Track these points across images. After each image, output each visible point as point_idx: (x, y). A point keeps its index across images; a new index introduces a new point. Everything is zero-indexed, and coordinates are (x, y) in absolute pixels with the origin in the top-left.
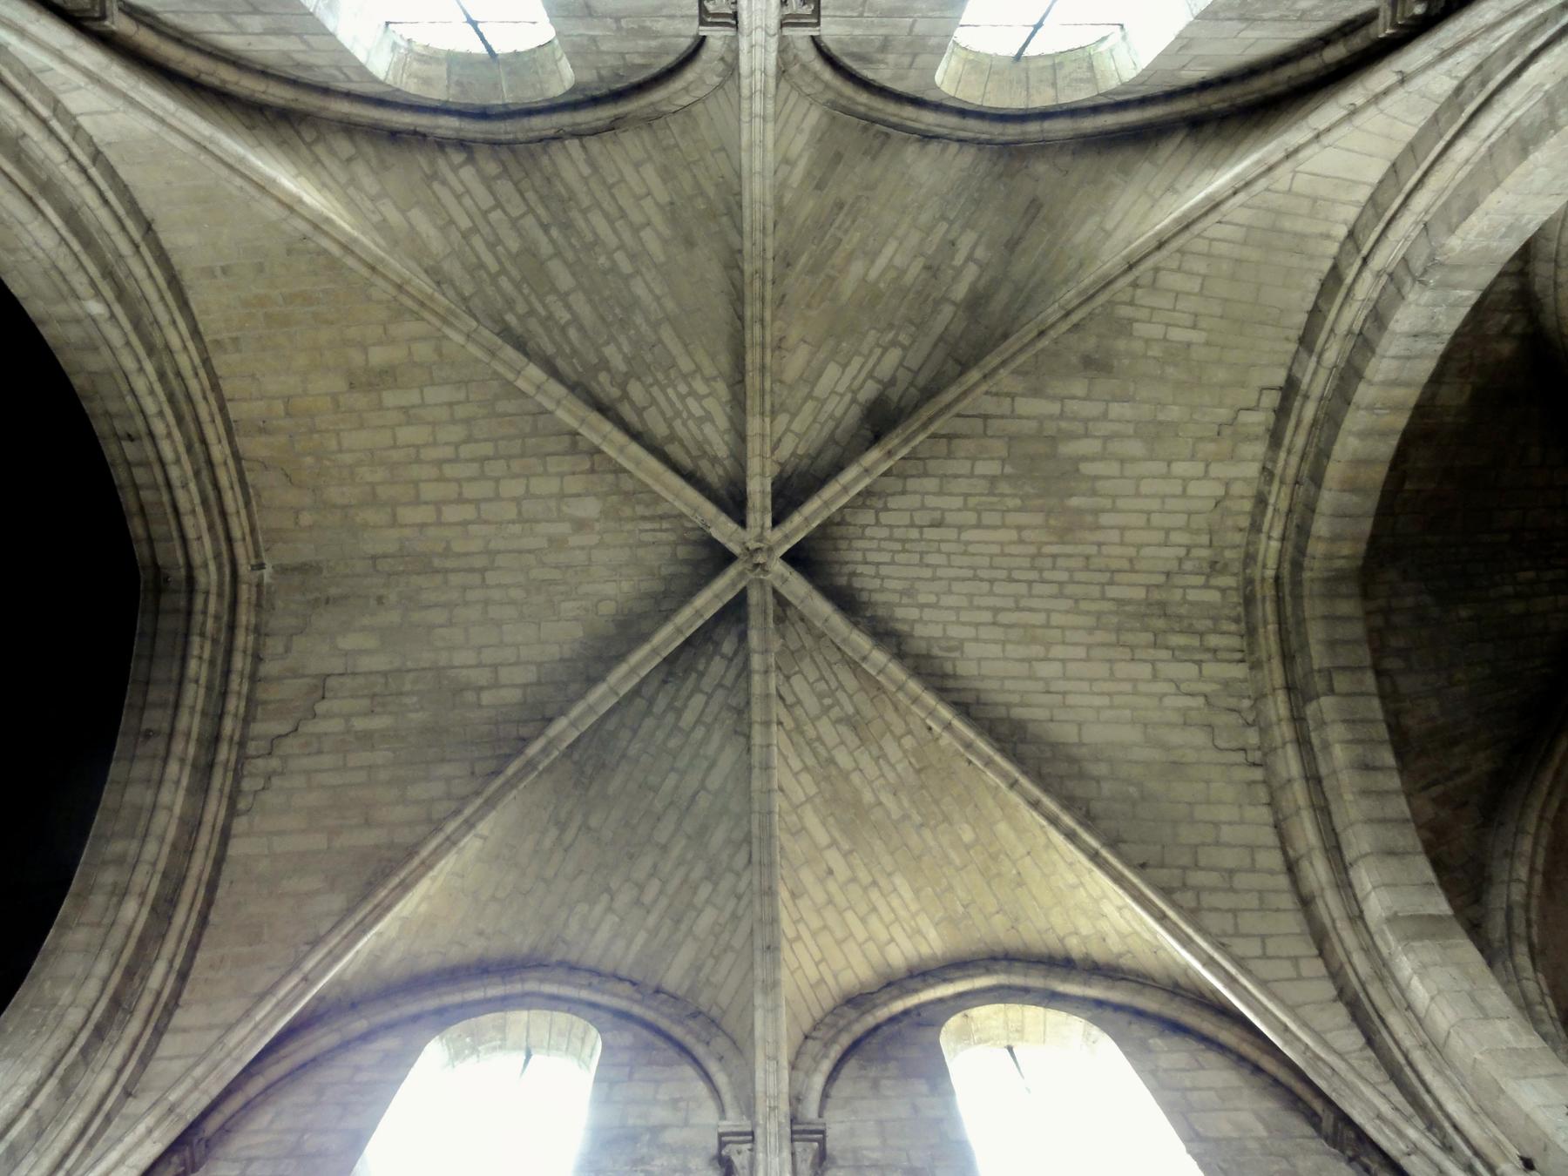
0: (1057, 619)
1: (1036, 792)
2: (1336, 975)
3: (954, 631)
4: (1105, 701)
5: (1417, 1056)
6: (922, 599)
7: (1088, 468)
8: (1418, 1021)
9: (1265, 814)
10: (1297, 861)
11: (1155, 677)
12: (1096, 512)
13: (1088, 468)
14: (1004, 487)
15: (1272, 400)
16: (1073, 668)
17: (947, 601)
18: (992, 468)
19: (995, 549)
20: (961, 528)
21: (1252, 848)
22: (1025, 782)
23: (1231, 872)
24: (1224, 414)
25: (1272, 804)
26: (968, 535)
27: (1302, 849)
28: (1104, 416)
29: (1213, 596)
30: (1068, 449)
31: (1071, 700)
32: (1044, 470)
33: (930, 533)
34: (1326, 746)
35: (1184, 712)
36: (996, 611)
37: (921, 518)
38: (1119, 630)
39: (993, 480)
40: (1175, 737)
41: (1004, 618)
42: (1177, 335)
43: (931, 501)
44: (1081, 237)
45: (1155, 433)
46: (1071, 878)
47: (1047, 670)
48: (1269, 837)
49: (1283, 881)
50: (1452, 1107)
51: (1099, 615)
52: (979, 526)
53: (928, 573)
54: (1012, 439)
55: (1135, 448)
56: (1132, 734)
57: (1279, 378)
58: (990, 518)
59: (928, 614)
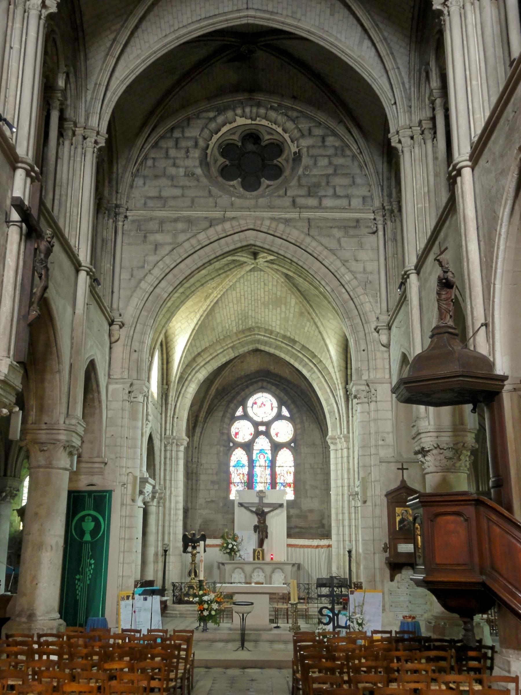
0: (243, 305)
1: (204, 315)
2: (184, 370)
3: (238, 290)
4: (225, 314)
5: (181, 395)
6: (246, 283)
7: (279, 309)
8: (185, 390)
9: (208, 345)
10: (201, 356)
11: (232, 321)
12: (268, 308)
13: (279, 309)
14: (274, 296)
15: (292, 337)
16: (232, 309)
17: (246, 288)
18: (279, 293)
19: (259, 293)
20: (264, 289)
21: (201, 346)
22: (206, 313)
23: (196, 346)
24: (290, 330)
25: (210, 346)
26: (262, 290)
27: (205, 357)
28: (290, 312)
29: (250, 323)
30: (283, 307)
31: (225, 310)
32: (277, 302)
33: (262, 284)
34: (224, 356)
35: (225, 326)
36: (244, 295)
37: (266, 282)
38: (241, 314)
39: (276, 294)
40: (220, 327)
41: (243, 297)
42: (306, 329)
43: (270, 284)
44: (329, 315)
45: (287, 320)
46: (184, 316)
47: (231, 305)
48: (203, 348)
49: (196, 353)
50: (178, 404)
51: (245, 310)
52: (264, 291)
53: (252, 283)
54: (286, 298)
55: (283, 315)
56: (219, 320)
57: (297, 339)
58: (266, 293)
59: (242, 285)
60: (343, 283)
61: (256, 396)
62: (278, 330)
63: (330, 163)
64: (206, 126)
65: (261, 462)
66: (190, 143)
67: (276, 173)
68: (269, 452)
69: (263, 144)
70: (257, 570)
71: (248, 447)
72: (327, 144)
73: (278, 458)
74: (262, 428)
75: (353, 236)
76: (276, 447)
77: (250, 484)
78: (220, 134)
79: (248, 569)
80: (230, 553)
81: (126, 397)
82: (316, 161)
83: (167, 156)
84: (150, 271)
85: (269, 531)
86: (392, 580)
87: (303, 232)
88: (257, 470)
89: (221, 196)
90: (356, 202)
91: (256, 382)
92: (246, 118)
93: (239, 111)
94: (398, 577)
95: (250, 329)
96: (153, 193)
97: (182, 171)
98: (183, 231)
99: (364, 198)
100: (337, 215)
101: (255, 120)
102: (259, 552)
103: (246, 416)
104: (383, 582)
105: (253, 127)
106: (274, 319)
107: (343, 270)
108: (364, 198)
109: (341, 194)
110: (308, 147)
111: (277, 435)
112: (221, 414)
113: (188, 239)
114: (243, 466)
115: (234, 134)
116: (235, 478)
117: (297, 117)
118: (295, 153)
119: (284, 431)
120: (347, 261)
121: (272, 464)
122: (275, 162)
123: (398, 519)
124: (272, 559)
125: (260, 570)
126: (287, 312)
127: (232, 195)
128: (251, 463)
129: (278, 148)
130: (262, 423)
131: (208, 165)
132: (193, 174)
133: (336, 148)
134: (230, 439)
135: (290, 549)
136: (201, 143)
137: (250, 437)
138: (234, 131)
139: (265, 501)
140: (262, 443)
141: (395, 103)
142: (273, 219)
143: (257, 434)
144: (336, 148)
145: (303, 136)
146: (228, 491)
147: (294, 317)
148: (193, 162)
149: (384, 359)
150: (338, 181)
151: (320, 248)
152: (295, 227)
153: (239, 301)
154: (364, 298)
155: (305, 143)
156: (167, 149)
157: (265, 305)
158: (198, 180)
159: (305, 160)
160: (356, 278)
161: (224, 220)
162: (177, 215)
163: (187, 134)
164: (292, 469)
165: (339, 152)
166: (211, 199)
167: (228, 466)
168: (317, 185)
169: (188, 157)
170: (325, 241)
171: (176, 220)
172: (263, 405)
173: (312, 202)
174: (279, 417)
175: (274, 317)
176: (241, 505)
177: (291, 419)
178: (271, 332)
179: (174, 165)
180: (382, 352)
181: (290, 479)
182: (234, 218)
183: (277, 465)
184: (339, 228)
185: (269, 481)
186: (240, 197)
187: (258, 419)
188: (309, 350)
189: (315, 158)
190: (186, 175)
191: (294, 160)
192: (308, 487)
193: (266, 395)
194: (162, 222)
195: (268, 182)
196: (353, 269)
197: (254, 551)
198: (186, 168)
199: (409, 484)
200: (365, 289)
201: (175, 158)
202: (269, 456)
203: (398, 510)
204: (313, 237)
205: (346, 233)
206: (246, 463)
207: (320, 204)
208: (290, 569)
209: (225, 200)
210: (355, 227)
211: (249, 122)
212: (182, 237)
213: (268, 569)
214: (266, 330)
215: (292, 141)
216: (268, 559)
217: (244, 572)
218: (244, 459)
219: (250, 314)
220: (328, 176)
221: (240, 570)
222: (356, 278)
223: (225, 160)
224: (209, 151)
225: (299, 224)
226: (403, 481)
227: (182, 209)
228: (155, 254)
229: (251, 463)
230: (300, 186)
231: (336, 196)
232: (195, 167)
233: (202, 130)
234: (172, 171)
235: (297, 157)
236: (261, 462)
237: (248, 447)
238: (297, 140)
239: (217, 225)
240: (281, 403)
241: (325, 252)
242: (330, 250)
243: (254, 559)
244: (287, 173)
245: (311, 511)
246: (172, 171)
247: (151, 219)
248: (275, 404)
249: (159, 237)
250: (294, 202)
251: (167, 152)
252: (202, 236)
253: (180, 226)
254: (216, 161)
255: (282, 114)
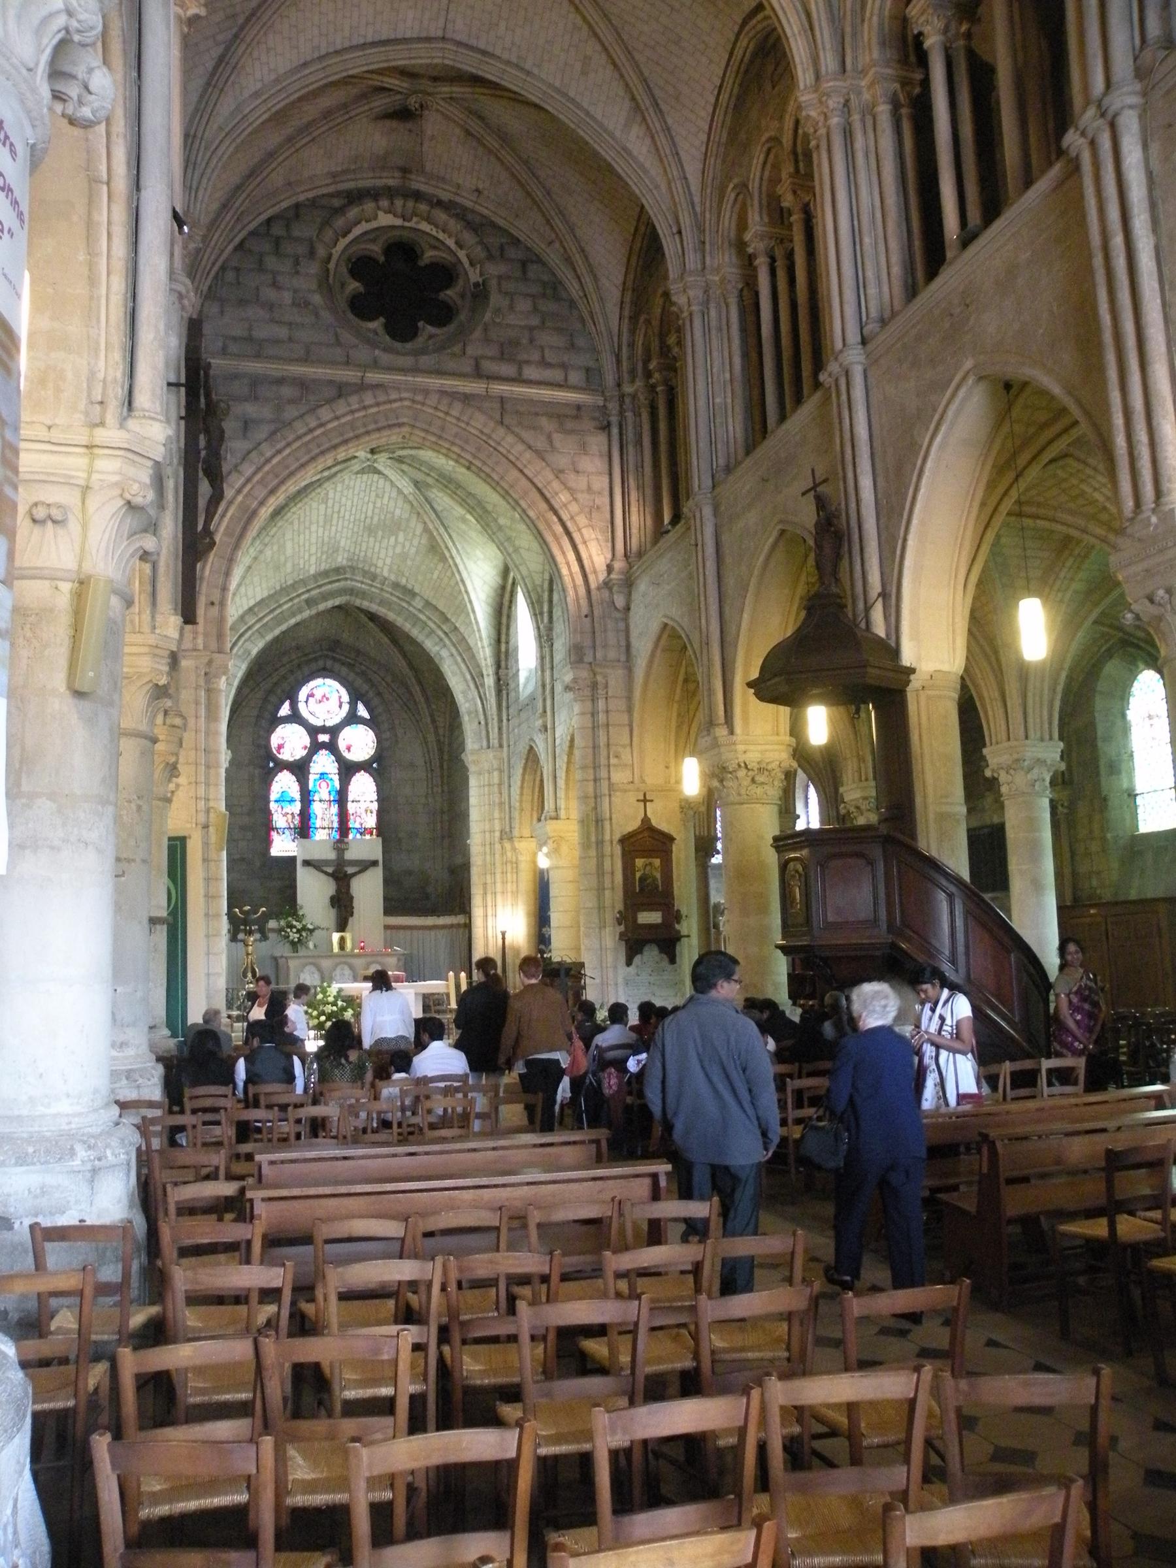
9: (265, 594)
13: (393, 539)
15: (409, 586)
18: (398, 512)
32: (394, 527)
37: (380, 492)
40: (289, 565)
42: (436, 574)
44: (478, 552)
47: (314, 528)
54: (408, 520)
55: (398, 550)
57: (417, 590)
60: (556, 506)
61: (312, 684)
62: (386, 574)
63: (535, 309)
64: (326, 223)
65: (323, 792)
66: (301, 250)
67: (443, 315)
68: (336, 778)
69: (421, 263)
71: (300, 769)
72: (531, 275)
73: (351, 788)
74: (324, 738)
75: (572, 432)
76: (348, 769)
77: (303, 829)
78: (351, 237)
81: (202, 682)
82: (512, 300)
83: (261, 268)
84: (236, 466)
85: (355, 904)
86: (629, 963)
87: (491, 418)
88: (317, 808)
89: (356, 346)
90: (575, 377)
91: (316, 659)
92: (395, 215)
93: (384, 203)
94: (637, 960)
95: (337, 570)
96: (238, 331)
97: (287, 297)
98: (291, 401)
99: (588, 370)
100: (547, 394)
101: (410, 220)
103: (295, 717)
104: (615, 967)
105: (405, 233)
106: (382, 555)
107: (556, 485)
108: (588, 370)
109: (553, 361)
110: (500, 277)
111: (349, 749)
112: (255, 713)
113: (302, 416)
114: (292, 801)
115: (374, 241)
116: (279, 820)
117: (482, 225)
118: (476, 285)
119: (360, 742)
120: (562, 471)
121: (342, 799)
122: (442, 296)
123: (638, 875)
126: (407, 544)
127: (374, 345)
128: (306, 797)
129: (446, 274)
130: (324, 729)
131: (330, 289)
132: (307, 304)
133: (545, 284)
134: (270, 756)
136: (321, 252)
137: (304, 753)
138: (371, 236)
139: (349, 855)
140: (324, 763)
141: (680, 232)
142: (443, 393)
143: (316, 747)
144: (545, 284)
145: (490, 257)
146: (268, 842)
147: (417, 552)
148: (306, 282)
149: (618, 631)
150: (547, 338)
151: (520, 447)
152: (479, 409)
153: (328, 520)
154: (588, 533)
155: (494, 270)
156: (261, 255)
157: (370, 530)
158: (317, 315)
159: (495, 299)
160: (575, 499)
161: (362, 387)
162: (279, 374)
163: (296, 233)
164: (375, 806)
165: (549, 292)
166: (339, 350)
167: (267, 801)
168: (515, 343)
169: (297, 273)
170: (527, 435)
171: (281, 381)
172: (324, 698)
173: (507, 369)
174: (352, 718)
175: (383, 552)
176: (307, 863)
177: (371, 723)
178: (374, 577)
179: (275, 285)
180: (616, 620)
181: (371, 821)
182: (379, 386)
183: (350, 798)
184: (550, 416)
185: (336, 825)
186: (385, 350)
187: (318, 723)
188: (436, 609)
189: (511, 295)
190: (294, 304)
191: (475, 296)
192: (401, 835)
193: (329, 681)
194: (256, 382)
195: (430, 329)
196: (571, 484)
198: (295, 291)
199: (654, 823)
200: (590, 519)
201: (275, 274)
202: (337, 785)
203: (639, 862)
204: (508, 427)
205: (561, 424)
206: (297, 796)
207: (520, 374)
209: (363, 353)
210: (576, 417)
211: (398, 222)
212: (291, 412)
214: (365, 573)
215: (472, 264)
218: (294, 790)
219: (342, 544)
220: (532, 329)
221: (313, 969)
222: (575, 499)
223: (357, 284)
224: (332, 266)
225: (487, 405)
226: (646, 820)
227: (291, 361)
228: (245, 436)
229: (306, 797)
230: (487, 340)
231: (544, 363)
232: (309, 291)
233: (320, 230)
234: (269, 294)
235: (480, 294)
236: (323, 792)
237: (300, 769)
238: (481, 263)
239: (350, 395)
240: (356, 696)
241: (528, 455)
242: (537, 452)
244: (463, 317)
245: (410, 873)
246: (269, 294)
247: (236, 376)
248: (346, 698)
249: (251, 409)
250: (477, 366)
251: (261, 262)
252: (325, 413)
253: (287, 391)
254: (343, 285)
255: (457, 216)
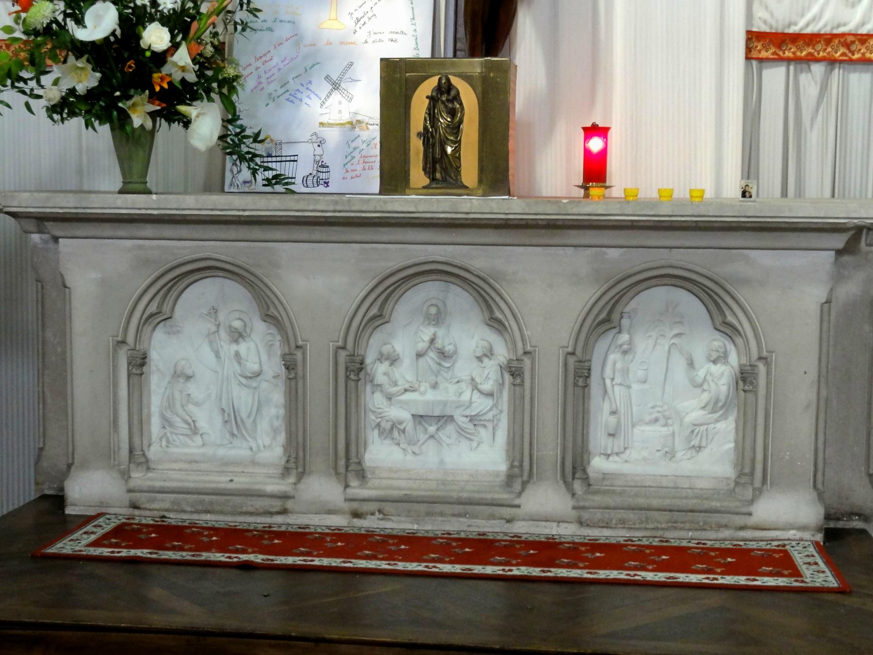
70: (427, 292)
79: (321, 281)
80: (97, 105)
102: (445, 94)
124: (595, 169)
125: (458, 298)
135: (775, 77)
197: (398, 78)
208: (813, 295)
213: (549, 290)
216: (551, 172)
217: (272, 313)
243: (393, 178)
